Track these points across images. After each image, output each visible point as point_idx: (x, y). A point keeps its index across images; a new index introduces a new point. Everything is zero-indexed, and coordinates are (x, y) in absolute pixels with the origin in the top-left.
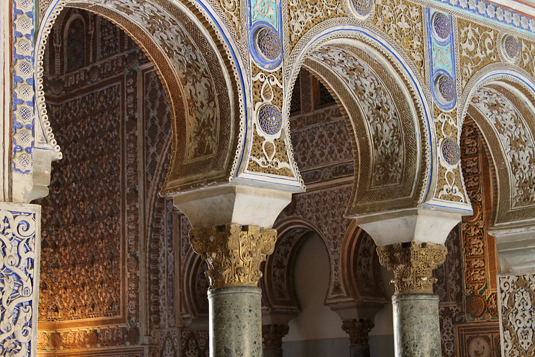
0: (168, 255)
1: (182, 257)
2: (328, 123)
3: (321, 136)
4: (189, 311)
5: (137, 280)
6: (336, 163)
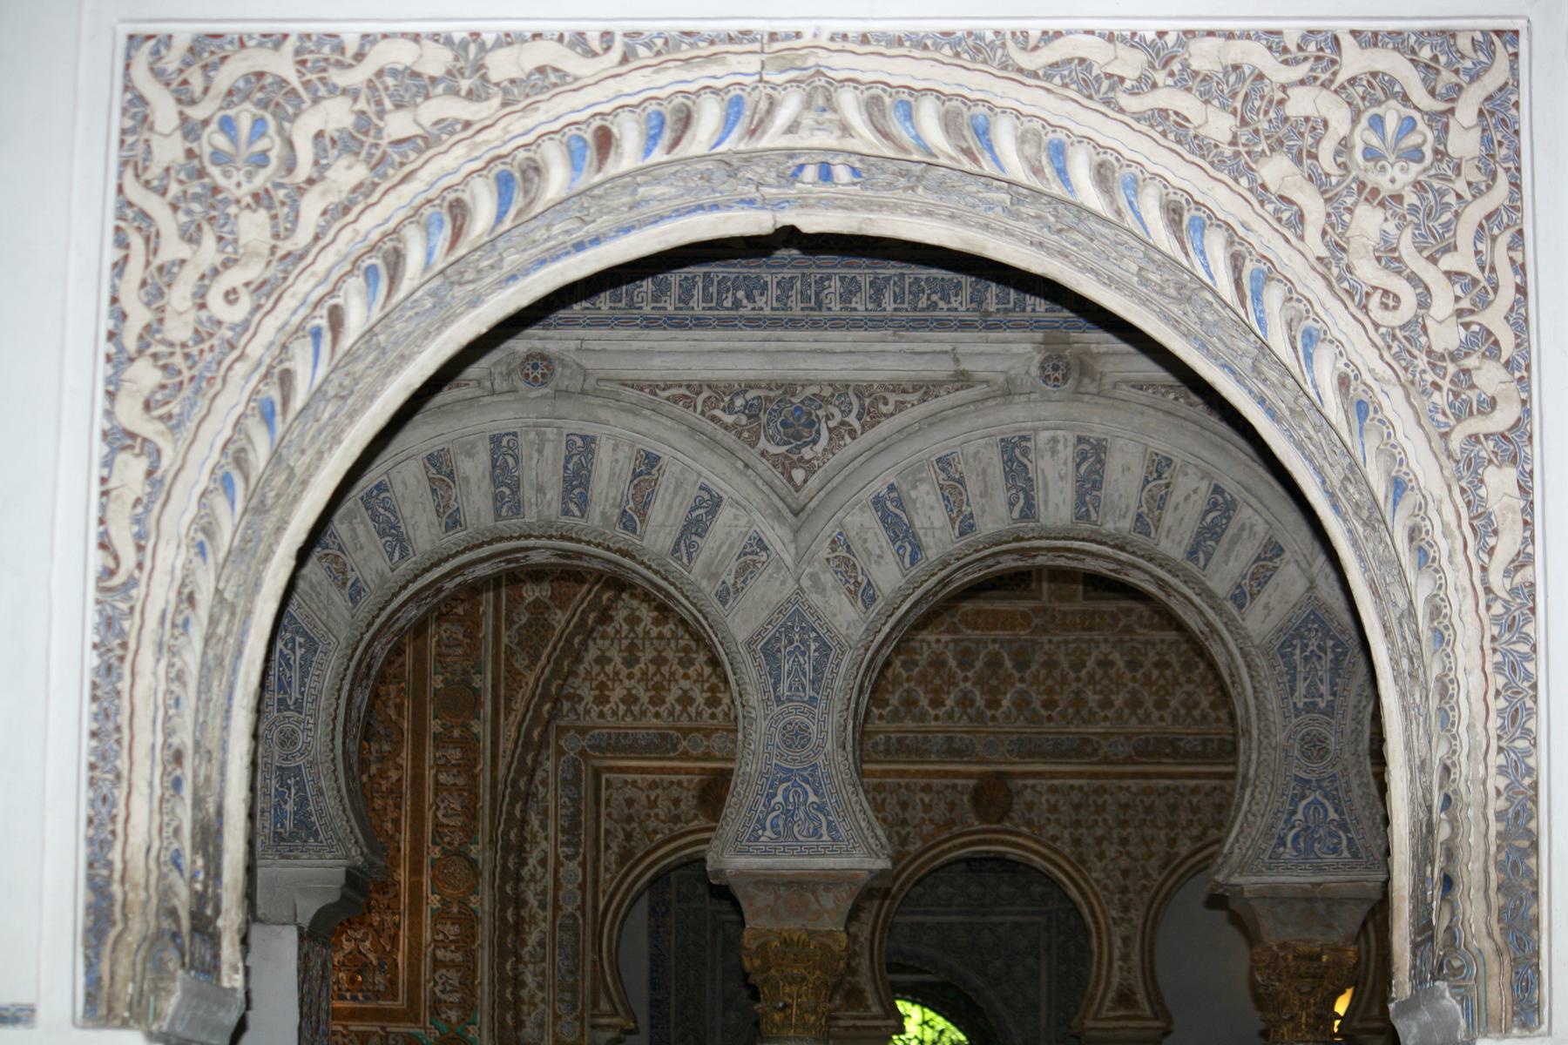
0: (558, 864)
1: (604, 876)
2: (1127, 638)
3: (1106, 663)
4: (619, 1007)
5: (468, 920)
6: (1147, 728)
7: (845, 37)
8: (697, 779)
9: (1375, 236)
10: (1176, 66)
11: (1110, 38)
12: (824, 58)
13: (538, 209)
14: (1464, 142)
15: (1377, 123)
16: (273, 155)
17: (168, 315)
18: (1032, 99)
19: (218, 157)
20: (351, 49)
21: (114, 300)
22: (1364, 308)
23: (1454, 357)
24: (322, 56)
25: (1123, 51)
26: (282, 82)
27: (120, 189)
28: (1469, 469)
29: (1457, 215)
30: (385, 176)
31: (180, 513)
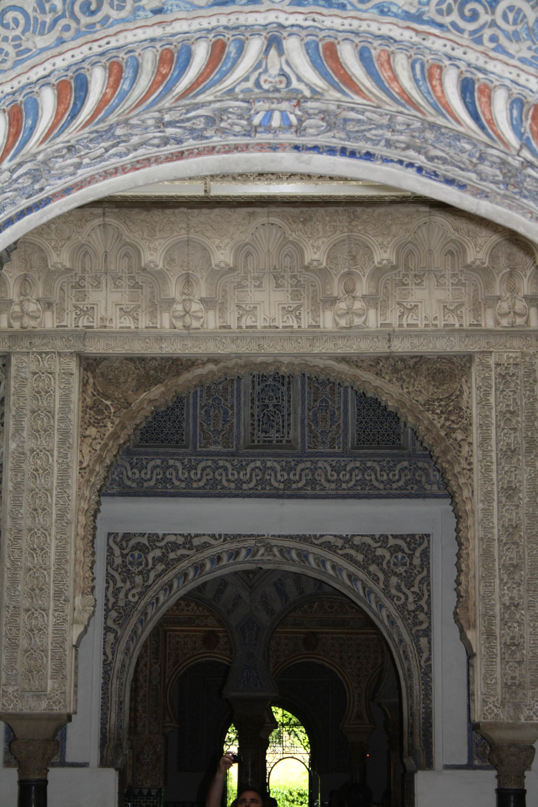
7: (274, 536)
8: (202, 634)
9: (395, 584)
10: (350, 543)
11: (335, 536)
12: (270, 541)
13: (204, 573)
14: (417, 561)
15: (396, 557)
16: (143, 563)
17: (119, 600)
18: (317, 551)
19: (131, 563)
20: (161, 537)
21: (106, 596)
22: (393, 600)
23: (413, 612)
24: (154, 538)
25: (338, 540)
26: (145, 545)
27: (107, 570)
28: (416, 638)
29: (415, 578)
30: (169, 568)
31: (122, 646)
